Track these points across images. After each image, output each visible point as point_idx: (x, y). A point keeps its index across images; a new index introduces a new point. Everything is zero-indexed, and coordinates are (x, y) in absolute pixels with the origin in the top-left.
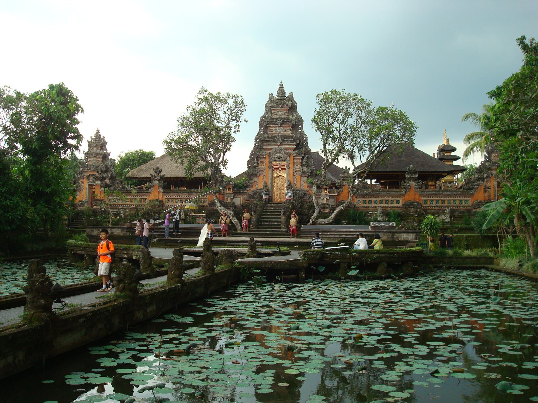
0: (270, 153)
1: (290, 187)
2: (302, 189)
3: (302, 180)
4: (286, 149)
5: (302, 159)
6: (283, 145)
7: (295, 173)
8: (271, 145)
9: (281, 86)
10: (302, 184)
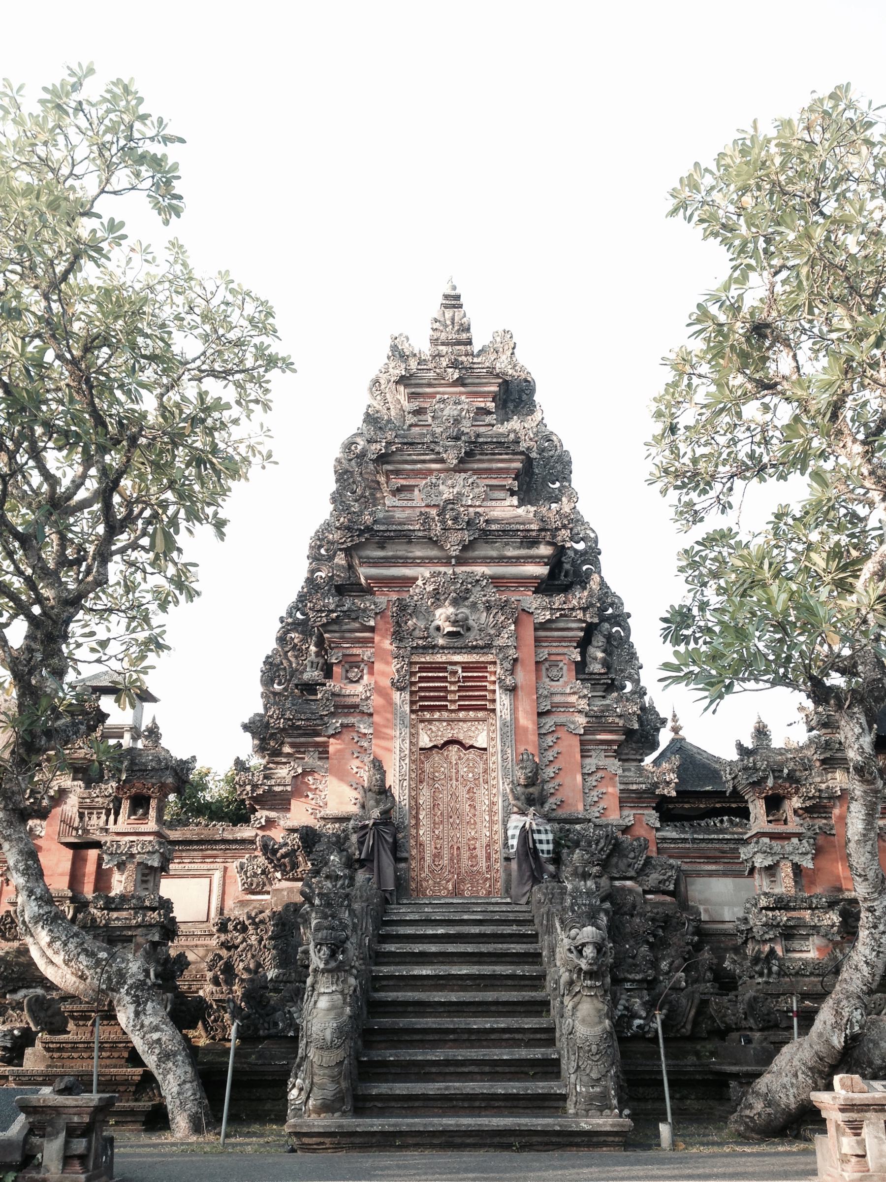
0: (402, 607)
1: (533, 793)
2: (595, 812)
3: (591, 763)
4: (497, 581)
5: (584, 644)
6: (474, 561)
7: (549, 721)
8: (406, 562)
9: (453, 301)
10: (594, 790)
